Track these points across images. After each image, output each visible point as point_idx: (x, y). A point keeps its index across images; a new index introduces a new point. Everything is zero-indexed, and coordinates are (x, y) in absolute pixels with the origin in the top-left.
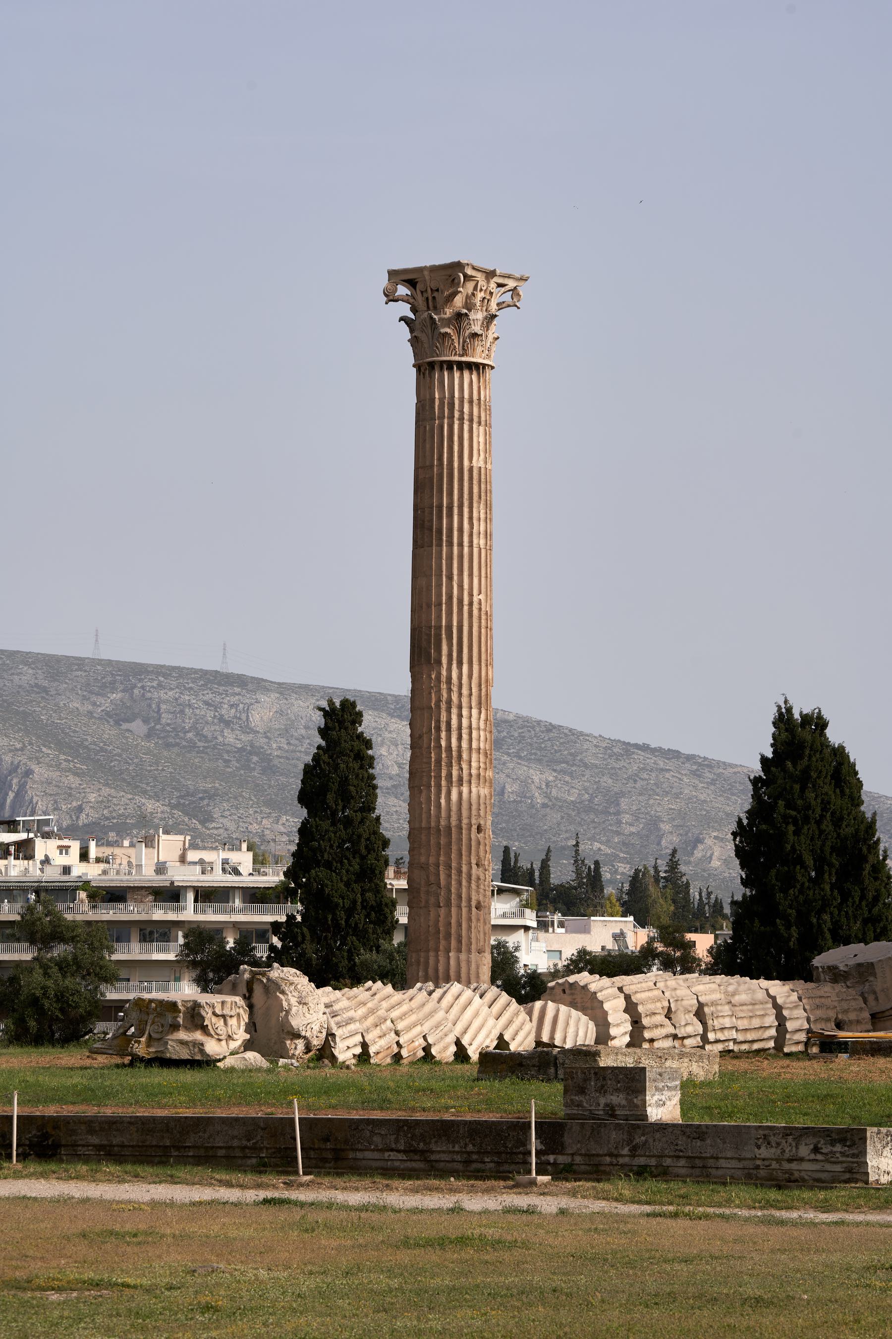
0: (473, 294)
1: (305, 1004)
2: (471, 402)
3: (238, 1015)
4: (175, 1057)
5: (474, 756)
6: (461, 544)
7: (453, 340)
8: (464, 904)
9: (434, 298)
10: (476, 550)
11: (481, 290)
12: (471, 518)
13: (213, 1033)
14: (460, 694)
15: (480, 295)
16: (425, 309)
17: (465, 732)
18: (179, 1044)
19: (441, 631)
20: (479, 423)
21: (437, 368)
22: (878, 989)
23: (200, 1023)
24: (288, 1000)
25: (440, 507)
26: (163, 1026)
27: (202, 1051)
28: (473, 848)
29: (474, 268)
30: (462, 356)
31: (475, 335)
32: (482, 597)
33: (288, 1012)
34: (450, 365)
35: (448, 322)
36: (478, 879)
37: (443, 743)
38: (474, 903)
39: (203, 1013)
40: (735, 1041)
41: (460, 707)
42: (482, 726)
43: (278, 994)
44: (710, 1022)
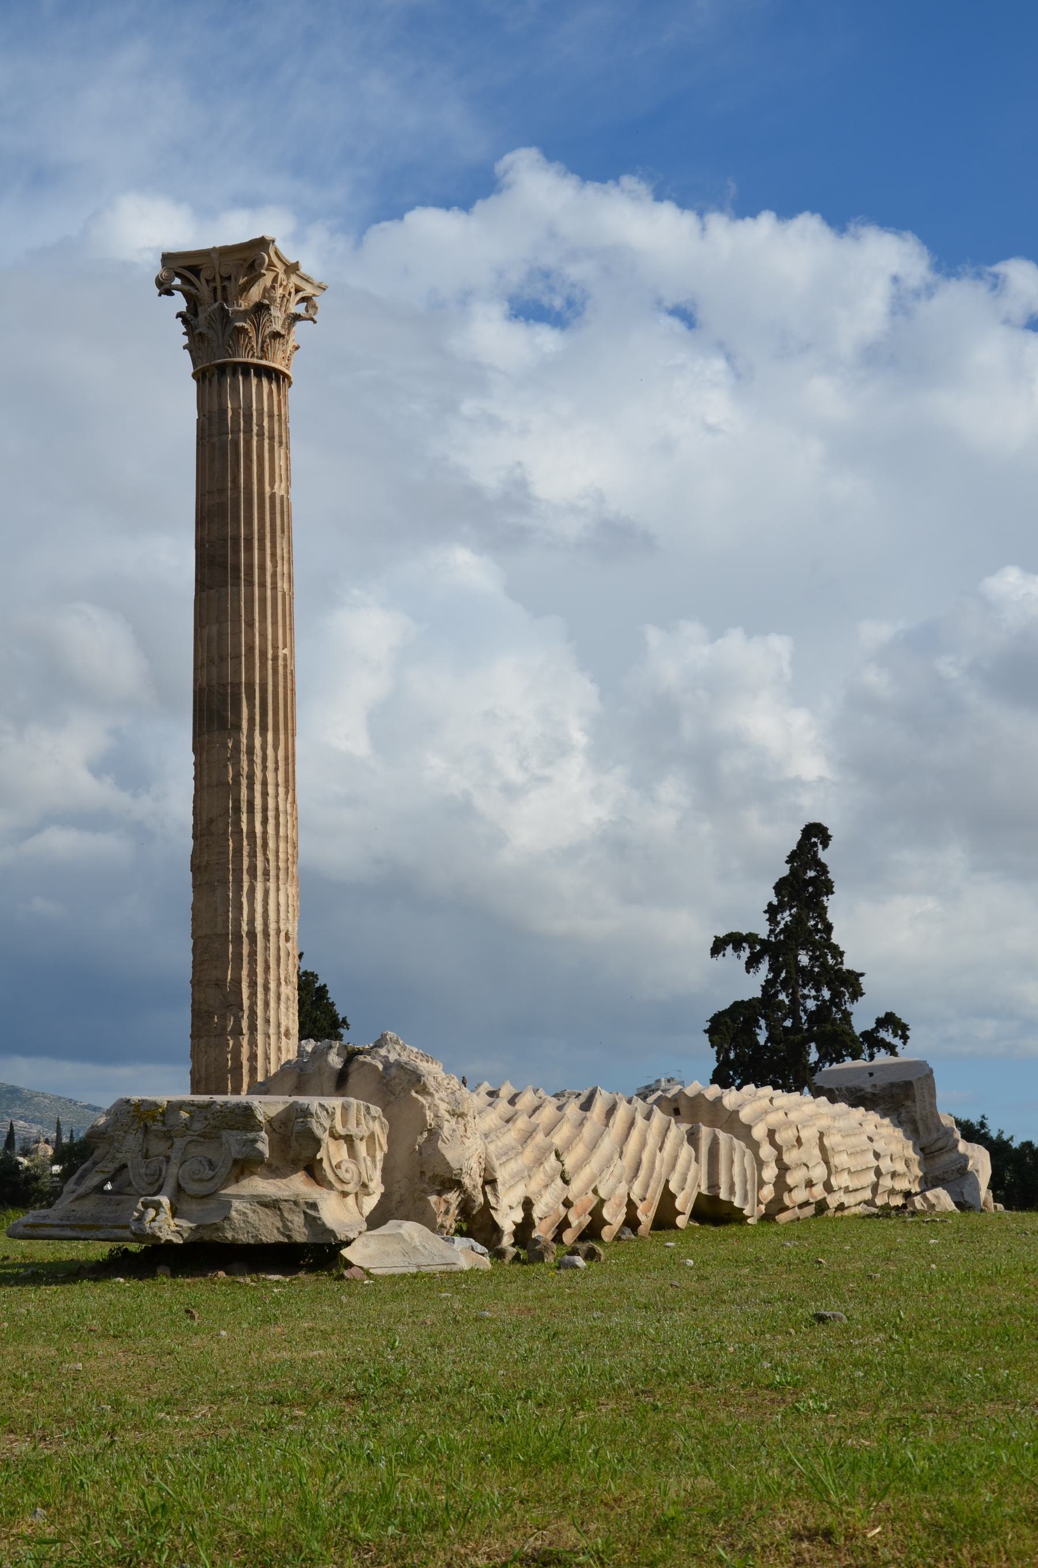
0: (273, 287)
1: (462, 1115)
2: (271, 416)
3: (372, 1136)
4: (244, 1238)
5: (282, 845)
6: (262, 585)
7: (250, 338)
8: (272, 1031)
9: (224, 288)
10: (280, 595)
11: (281, 285)
12: (274, 555)
13: (331, 1177)
14: (265, 768)
15: (280, 291)
16: (212, 301)
17: (271, 814)
18: (258, 1208)
19: (240, 689)
20: (281, 443)
21: (229, 371)
22: (918, 1117)
23: (306, 1154)
24: (434, 1107)
25: (236, 540)
26: (211, 1165)
27: (313, 1222)
28: (282, 960)
29: (277, 254)
30: (261, 359)
31: (276, 335)
32: (286, 651)
33: (434, 1134)
34: (246, 369)
35: (244, 315)
36: (288, 999)
37: (244, 827)
38: (283, 1030)
39: (318, 1132)
40: (847, 1190)
41: (265, 784)
42: (289, 810)
43: (414, 1094)
44: (831, 1160)
